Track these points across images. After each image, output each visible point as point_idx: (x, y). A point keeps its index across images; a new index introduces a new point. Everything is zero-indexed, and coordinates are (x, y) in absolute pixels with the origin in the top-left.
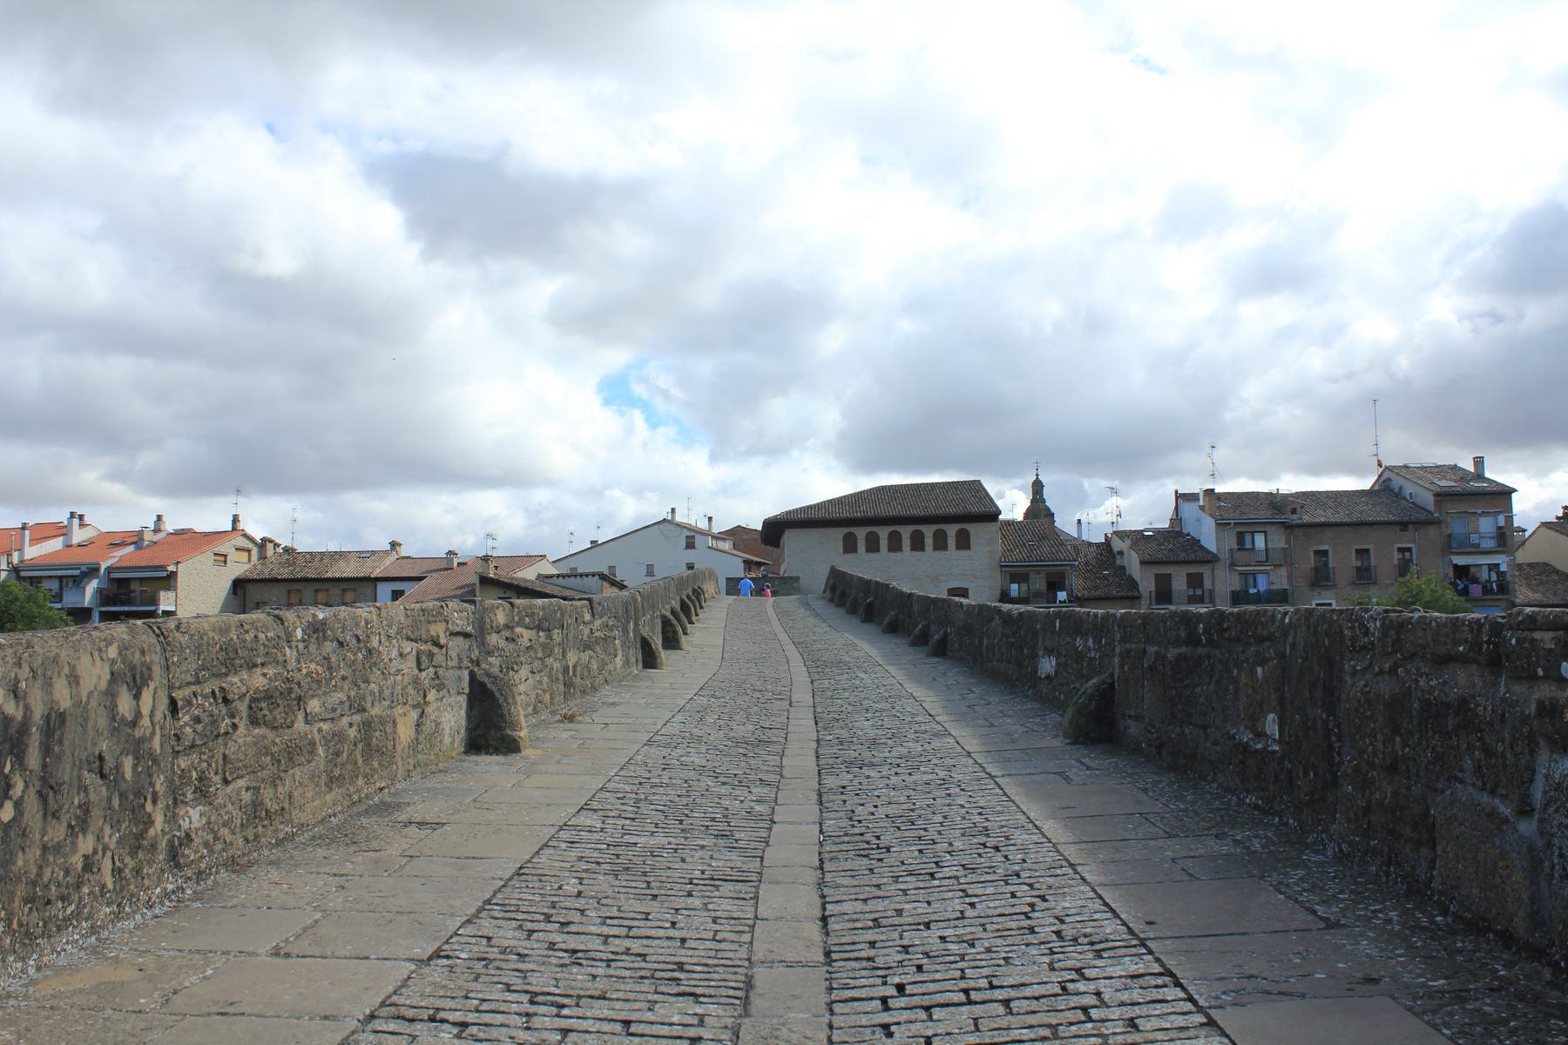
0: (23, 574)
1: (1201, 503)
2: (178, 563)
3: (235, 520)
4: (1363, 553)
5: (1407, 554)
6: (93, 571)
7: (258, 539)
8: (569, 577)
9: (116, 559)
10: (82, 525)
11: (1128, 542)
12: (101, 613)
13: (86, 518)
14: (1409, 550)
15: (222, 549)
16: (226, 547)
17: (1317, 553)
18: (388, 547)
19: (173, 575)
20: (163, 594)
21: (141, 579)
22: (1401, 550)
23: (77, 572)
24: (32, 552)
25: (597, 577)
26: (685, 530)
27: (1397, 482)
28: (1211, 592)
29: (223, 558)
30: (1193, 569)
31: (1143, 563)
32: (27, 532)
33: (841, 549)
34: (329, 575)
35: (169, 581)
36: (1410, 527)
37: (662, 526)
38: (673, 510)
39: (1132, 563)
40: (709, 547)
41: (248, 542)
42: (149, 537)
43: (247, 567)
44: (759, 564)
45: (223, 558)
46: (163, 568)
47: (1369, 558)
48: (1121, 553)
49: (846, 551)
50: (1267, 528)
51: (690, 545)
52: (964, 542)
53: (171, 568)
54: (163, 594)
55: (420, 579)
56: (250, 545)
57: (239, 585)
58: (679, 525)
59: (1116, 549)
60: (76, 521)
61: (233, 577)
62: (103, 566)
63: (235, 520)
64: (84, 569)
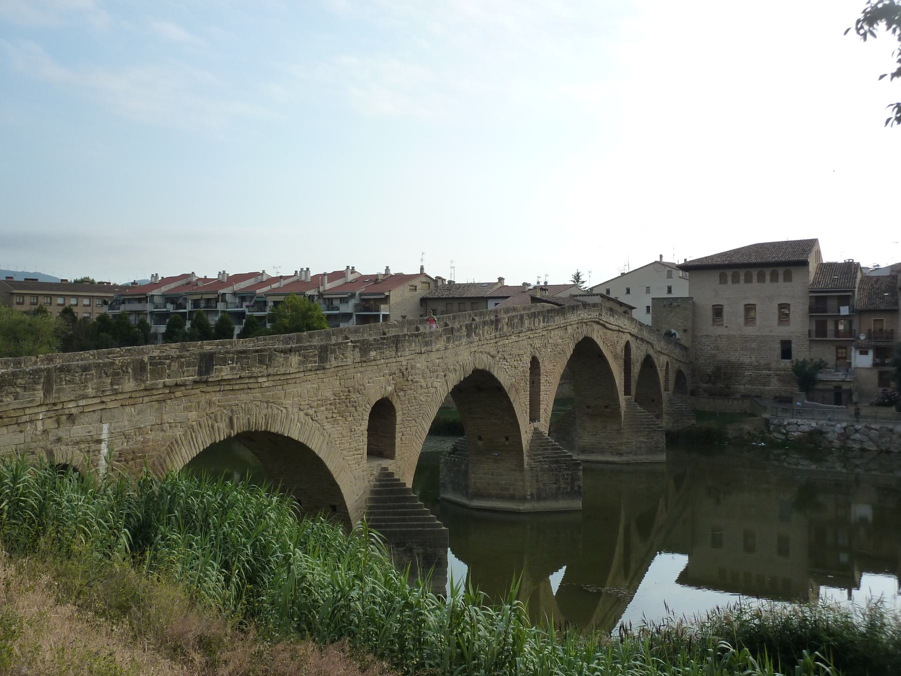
0: (325, 297)
2: (390, 291)
3: (422, 268)
6: (353, 296)
8: (586, 296)
12: (356, 315)
13: (355, 269)
18: (497, 281)
19: (388, 297)
20: (382, 306)
21: (375, 299)
23: (346, 296)
24: (328, 286)
25: (599, 296)
26: (667, 267)
32: (326, 277)
34: (465, 296)
35: (386, 300)
37: (654, 265)
38: (661, 256)
40: (680, 277)
41: (428, 279)
45: (414, 288)
46: (382, 294)
49: (720, 284)
51: (670, 275)
52: (788, 278)
53: (387, 294)
54: (382, 306)
55: (507, 297)
57: (424, 301)
62: (357, 293)
63: (422, 268)
64: (349, 294)
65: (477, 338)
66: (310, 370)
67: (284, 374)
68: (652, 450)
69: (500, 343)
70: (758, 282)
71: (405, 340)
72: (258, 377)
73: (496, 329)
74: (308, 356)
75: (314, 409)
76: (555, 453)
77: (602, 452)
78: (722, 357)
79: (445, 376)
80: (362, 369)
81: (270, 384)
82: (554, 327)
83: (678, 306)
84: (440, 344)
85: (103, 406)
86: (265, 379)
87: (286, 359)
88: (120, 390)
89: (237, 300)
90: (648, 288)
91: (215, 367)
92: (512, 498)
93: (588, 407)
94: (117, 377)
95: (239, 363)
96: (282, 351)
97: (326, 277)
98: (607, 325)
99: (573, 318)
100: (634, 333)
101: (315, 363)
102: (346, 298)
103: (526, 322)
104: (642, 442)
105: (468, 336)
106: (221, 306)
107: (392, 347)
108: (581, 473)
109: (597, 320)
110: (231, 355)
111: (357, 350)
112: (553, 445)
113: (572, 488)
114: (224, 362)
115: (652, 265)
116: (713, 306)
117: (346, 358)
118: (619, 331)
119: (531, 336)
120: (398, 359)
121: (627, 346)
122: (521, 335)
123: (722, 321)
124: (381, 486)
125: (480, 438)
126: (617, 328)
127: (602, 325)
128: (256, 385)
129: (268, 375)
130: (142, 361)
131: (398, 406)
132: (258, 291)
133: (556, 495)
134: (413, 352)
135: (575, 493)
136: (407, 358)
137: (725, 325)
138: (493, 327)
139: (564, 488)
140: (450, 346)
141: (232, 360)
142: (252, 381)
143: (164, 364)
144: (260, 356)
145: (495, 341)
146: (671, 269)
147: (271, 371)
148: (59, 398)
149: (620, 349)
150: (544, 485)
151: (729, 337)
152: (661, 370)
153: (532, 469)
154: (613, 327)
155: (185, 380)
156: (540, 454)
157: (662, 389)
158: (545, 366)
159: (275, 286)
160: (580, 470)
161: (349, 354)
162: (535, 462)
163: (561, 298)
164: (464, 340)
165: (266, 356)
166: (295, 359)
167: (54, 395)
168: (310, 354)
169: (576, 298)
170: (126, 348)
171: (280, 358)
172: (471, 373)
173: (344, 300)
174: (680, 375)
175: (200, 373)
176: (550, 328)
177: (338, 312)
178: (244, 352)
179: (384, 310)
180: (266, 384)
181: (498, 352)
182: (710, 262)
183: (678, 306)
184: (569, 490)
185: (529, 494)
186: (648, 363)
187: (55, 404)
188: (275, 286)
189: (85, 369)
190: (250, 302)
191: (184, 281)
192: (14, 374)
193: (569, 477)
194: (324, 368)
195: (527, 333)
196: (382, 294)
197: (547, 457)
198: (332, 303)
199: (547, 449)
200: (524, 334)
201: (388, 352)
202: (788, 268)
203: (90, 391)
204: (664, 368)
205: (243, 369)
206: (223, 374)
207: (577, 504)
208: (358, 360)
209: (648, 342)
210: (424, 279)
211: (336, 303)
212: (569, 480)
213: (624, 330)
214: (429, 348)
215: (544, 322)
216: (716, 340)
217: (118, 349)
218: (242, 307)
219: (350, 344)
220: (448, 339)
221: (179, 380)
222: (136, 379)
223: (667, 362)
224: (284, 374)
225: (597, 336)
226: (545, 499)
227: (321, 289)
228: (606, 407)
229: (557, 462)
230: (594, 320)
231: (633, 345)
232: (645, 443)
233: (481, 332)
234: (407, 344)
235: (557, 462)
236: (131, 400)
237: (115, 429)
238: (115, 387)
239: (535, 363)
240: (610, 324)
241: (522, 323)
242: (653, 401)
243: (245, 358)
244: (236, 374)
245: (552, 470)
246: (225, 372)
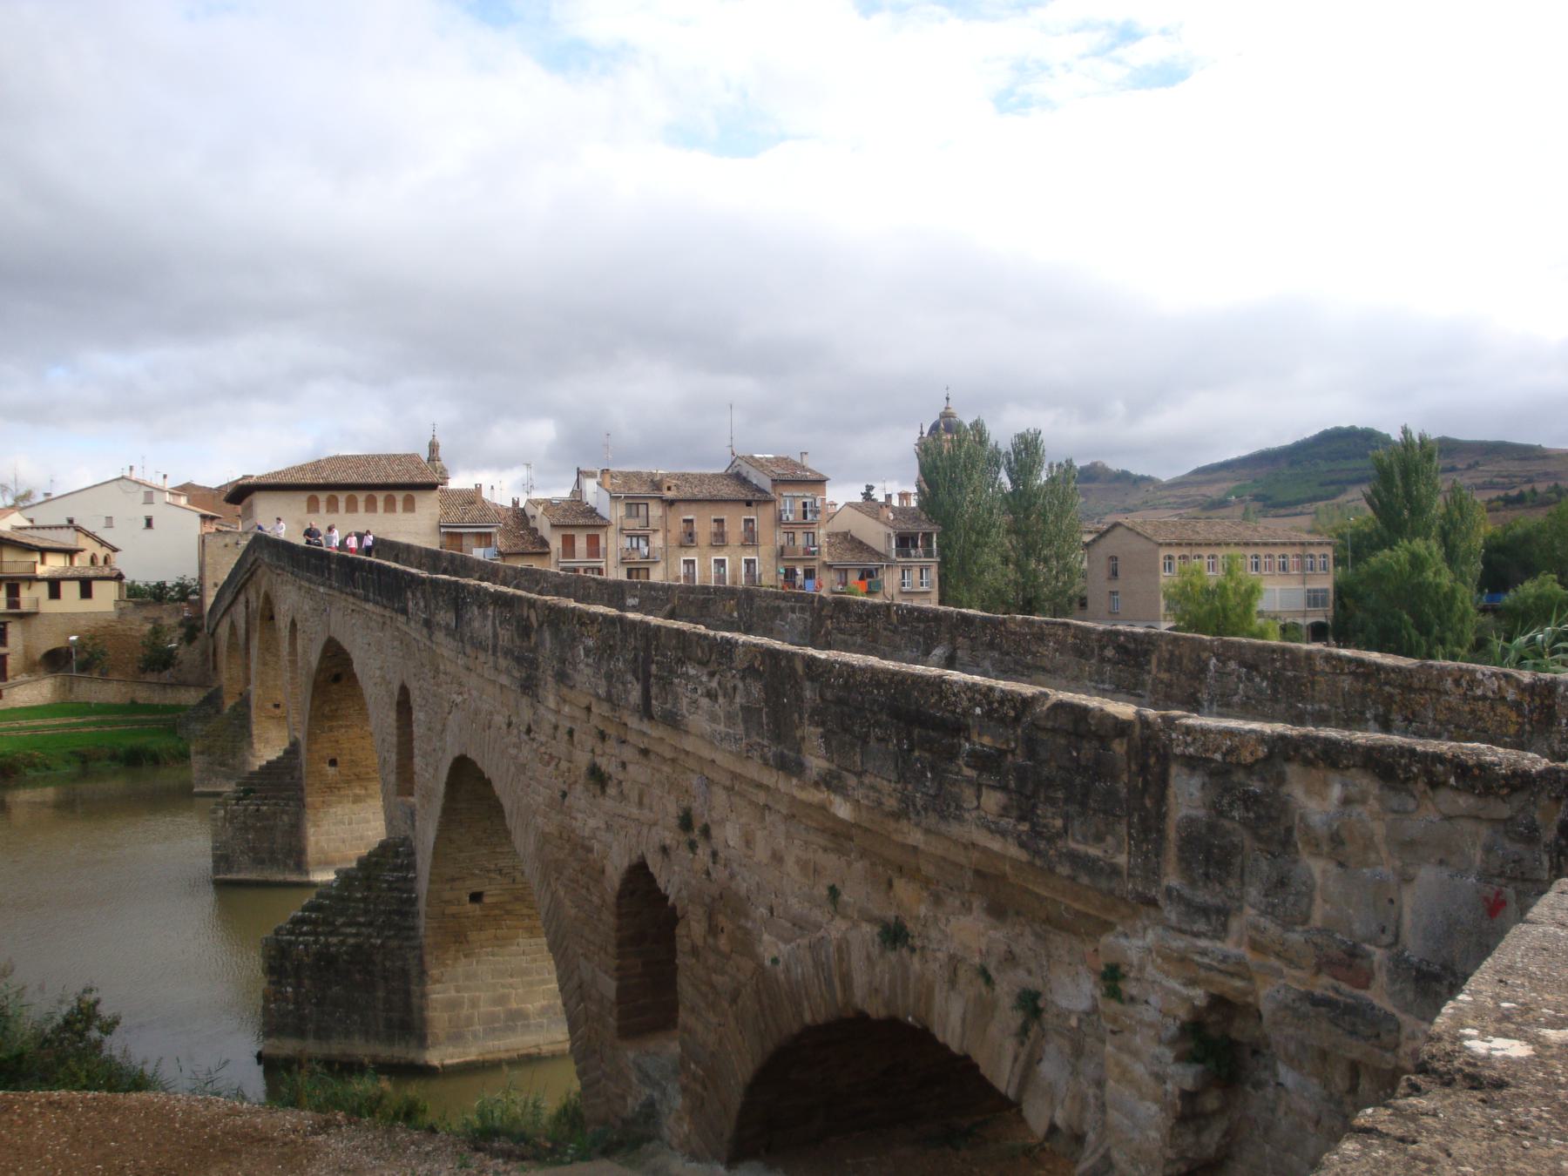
1: (599, 479)
4: (720, 522)
5: (751, 524)
11: (541, 509)
14: (752, 520)
17: (685, 521)
22: (747, 521)
27: (746, 470)
28: (606, 549)
30: (591, 532)
31: (553, 526)
33: (305, 510)
36: (754, 504)
37: (121, 483)
38: (131, 468)
39: (543, 526)
44: (213, 518)
47: (723, 526)
48: (534, 517)
50: (648, 502)
51: (149, 499)
52: (409, 506)
58: (136, 482)
59: (529, 513)
70: (366, 511)
90: (109, 519)
93: (277, 706)
125: (333, 763)
146: (149, 490)
202: (410, 493)
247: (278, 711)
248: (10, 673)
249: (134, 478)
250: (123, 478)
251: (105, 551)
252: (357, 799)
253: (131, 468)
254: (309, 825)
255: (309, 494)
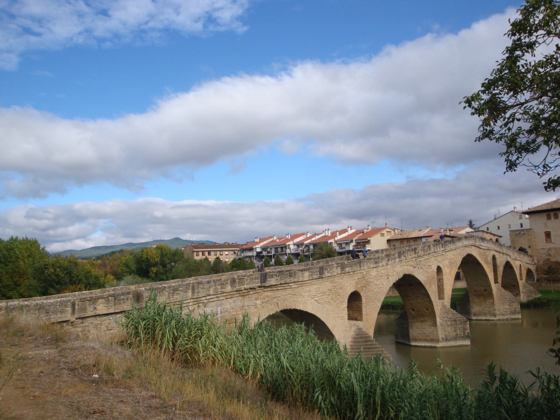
0: (338, 243)
6: (352, 241)
7: (393, 229)
9: (357, 238)
10: (351, 230)
15: (382, 232)
16: (384, 232)
19: (369, 240)
20: (367, 245)
21: (363, 242)
23: (348, 241)
24: (339, 237)
29: (383, 235)
40: (526, 218)
42: (365, 231)
43: (390, 236)
51: (521, 218)
53: (369, 239)
54: (367, 245)
55: (431, 236)
56: (390, 230)
58: (516, 212)
60: (349, 229)
61: (387, 239)
64: (350, 240)
65: (404, 258)
66: (315, 279)
67: (302, 281)
68: (514, 313)
69: (418, 260)
71: (364, 261)
72: (289, 283)
73: (415, 253)
74: (314, 272)
75: (319, 298)
76: (454, 316)
77: (485, 314)
78: (553, 260)
79: (388, 278)
80: (342, 277)
81: (297, 286)
82: (449, 250)
83: (524, 234)
84: (384, 263)
85: (218, 299)
86: (293, 284)
87: (303, 275)
88: (225, 292)
89: (296, 247)
90: (509, 225)
91: (268, 279)
92: (432, 340)
94: (223, 285)
95: (279, 278)
96: (300, 270)
97: (338, 233)
98: (480, 247)
99: (459, 244)
100: (498, 250)
101: (317, 275)
102: (348, 242)
103: (432, 248)
104: (507, 308)
105: (399, 257)
106: (288, 251)
107: (358, 265)
108: (468, 326)
109: (474, 244)
110: (275, 273)
111: (339, 268)
112: (452, 312)
113: (464, 334)
114: (272, 277)
115: (510, 213)
116: (545, 232)
117: (333, 272)
118: (488, 249)
119: (436, 255)
120: (361, 271)
121: (494, 258)
122: (429, 255)
123: (551, 240)
124: (357, 335)
125: (413, 310)
126: (487, 248)
127: (477, 247)
128: (289, 287)
129: (294, 282)
130: (234, 278)
131: (362, 294)
132: (305, 242)
133: (455, 338)
134: (369, 267)
135: (465, 337)
136: (366, 270)
137: (553, 242)
138: (413, 252)
139: (460, 334)
140: (390, 262)
141: (276, 275)
142: (286, 285)
143: (244, 279)
144: (290, 273)
145: (415, 259)
147: (296, 280)
148: (198, 295)
149: (490, 259)
150: (449, 333)
151: (555, 249)
152: (517, 269)
153: (441, 325)
154: (484, 248)
155: (255, 286)
156: (445, 317)
157: (519, 280)
158: (445, 270)
159: (313, 239)
160: (467, 324)
161: (334, 269)
162: (443, 321)
163: (460, 234)
164: (397, 260)
165: (292, 273)
166: (307, 274)
167: (196, 294)
168: (315, 271)
169: (469, 234)
170: (230, 272)
171: (300, 274)
172: (402, 276)
173: (347, 244)
174: (529, 272)
175: (261, 283)
176: (446, 251)
177: (345, 250)
178: (282, 272)
179: (368, 247)
180: (294, 286)
181: (417, 265)
182: (535, 210)
183: (524, 234)
184: (462, 335)
185: (441, 338)
186: (508, 266)
187: (197, 298)
188: (313, 239)
189: (209, 282)
190: (302, 248)
191: (271, 240)
192: (179, 286)
193: (462, 328)
194: (322, 278)
195: (433, 254)
196: (367, 239)
197: (450, 318)
198: (342, 246)
199: (449, 314)
200: (431, 255)
201: (355, 268)
203: (211, 292)
204: (519, 268)
205: (281, 279)
206: (272, 282)
207: (468, 342)
208: (340, 273)
209: (507, 255)
210: (388, 230)
211: (343, 246)
212: (462, 330)
213: (491, 249)
214: (378, 265)
215: (442, 247)
216: (549, 250)
217: (226, 273)
218: (298, 251)
219: (335, 265)
220: (388, 260)
221: (251, 286)
222: (231, 286)
223: (520, 265)
224: (302, 281)
225: (475, 253)
226: (450, 340)
227: (336, 239)
228: (485, 290)
229: (455, 321)
230: (472, 244)
231: (497, 256)
232: (509, 309)
233: (406, 255)
234: (365, 263)
235: (455, 321)
236: (230, 296)
237: (223, 309)
238: (223, 290)
239: (439, 269)
240: (482, 246)
241: (430, 249)
242: (514, 286)
243: (283, 274)
244: (278, 282)
245: (453, 325)
246: (273, 281)
247: (476, 293)
248: (461, 278)
249: (516, 211)
250: (512, 211)
251: (496, 237)
252: (422, 322)
253: (515, 208)
254: (410, 328)
255: (547, 213)
